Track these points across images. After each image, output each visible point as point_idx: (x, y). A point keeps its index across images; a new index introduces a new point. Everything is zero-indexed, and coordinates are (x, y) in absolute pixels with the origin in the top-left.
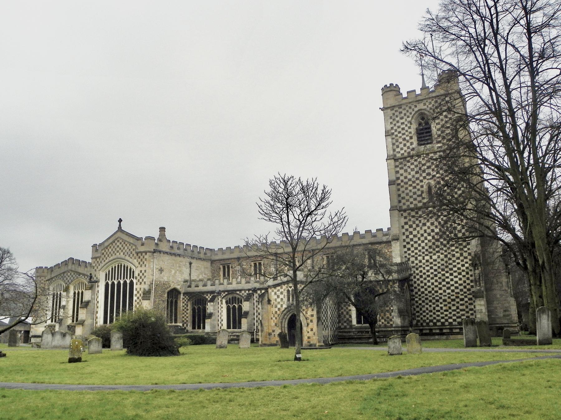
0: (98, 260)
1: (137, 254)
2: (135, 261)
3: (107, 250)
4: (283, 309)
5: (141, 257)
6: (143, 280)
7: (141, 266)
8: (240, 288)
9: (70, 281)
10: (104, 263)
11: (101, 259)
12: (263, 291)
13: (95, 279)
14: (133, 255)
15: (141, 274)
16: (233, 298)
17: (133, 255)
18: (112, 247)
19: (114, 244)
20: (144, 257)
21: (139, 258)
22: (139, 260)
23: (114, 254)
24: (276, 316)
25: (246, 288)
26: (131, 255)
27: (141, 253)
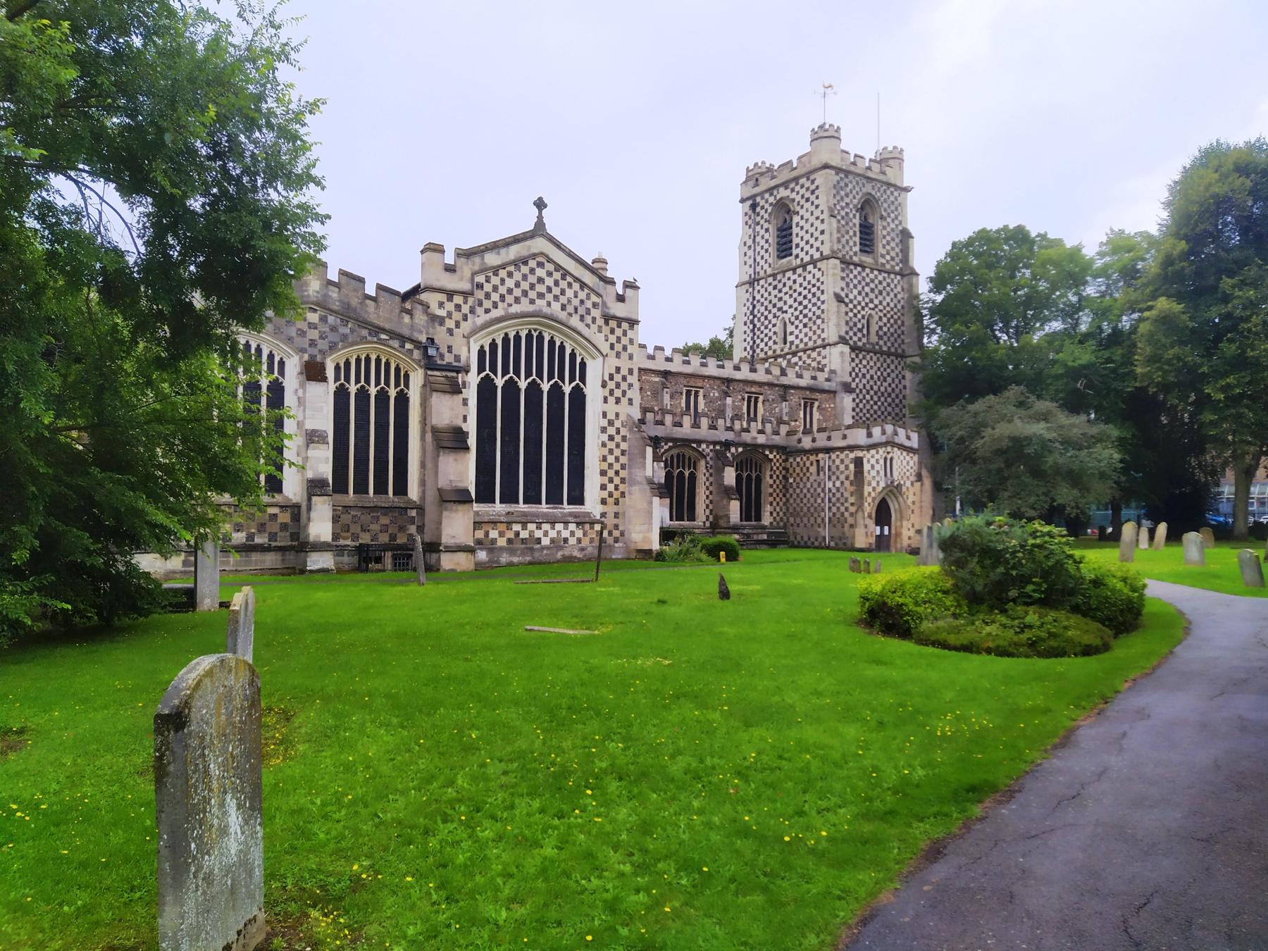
0: (458, 299)
1: (607, 323)
4: (879, 489)
5: (619, 332)
6: (624, 393)
8: (697, 437)
9: (323, 345)
10: (482, 318)
11: (471, 300)
12: (740, 450)
13: (449, 358)
14: (594, 320)
15: (618, 378)
17: (594, 320)
18: (517, 276)
19: (525, 269)
20: (625, 334)
21: (612, 331)
22: (613, 339)
23: (524, 301)
24: (870, 500)
25: (710, 439)
27: (620, 321)
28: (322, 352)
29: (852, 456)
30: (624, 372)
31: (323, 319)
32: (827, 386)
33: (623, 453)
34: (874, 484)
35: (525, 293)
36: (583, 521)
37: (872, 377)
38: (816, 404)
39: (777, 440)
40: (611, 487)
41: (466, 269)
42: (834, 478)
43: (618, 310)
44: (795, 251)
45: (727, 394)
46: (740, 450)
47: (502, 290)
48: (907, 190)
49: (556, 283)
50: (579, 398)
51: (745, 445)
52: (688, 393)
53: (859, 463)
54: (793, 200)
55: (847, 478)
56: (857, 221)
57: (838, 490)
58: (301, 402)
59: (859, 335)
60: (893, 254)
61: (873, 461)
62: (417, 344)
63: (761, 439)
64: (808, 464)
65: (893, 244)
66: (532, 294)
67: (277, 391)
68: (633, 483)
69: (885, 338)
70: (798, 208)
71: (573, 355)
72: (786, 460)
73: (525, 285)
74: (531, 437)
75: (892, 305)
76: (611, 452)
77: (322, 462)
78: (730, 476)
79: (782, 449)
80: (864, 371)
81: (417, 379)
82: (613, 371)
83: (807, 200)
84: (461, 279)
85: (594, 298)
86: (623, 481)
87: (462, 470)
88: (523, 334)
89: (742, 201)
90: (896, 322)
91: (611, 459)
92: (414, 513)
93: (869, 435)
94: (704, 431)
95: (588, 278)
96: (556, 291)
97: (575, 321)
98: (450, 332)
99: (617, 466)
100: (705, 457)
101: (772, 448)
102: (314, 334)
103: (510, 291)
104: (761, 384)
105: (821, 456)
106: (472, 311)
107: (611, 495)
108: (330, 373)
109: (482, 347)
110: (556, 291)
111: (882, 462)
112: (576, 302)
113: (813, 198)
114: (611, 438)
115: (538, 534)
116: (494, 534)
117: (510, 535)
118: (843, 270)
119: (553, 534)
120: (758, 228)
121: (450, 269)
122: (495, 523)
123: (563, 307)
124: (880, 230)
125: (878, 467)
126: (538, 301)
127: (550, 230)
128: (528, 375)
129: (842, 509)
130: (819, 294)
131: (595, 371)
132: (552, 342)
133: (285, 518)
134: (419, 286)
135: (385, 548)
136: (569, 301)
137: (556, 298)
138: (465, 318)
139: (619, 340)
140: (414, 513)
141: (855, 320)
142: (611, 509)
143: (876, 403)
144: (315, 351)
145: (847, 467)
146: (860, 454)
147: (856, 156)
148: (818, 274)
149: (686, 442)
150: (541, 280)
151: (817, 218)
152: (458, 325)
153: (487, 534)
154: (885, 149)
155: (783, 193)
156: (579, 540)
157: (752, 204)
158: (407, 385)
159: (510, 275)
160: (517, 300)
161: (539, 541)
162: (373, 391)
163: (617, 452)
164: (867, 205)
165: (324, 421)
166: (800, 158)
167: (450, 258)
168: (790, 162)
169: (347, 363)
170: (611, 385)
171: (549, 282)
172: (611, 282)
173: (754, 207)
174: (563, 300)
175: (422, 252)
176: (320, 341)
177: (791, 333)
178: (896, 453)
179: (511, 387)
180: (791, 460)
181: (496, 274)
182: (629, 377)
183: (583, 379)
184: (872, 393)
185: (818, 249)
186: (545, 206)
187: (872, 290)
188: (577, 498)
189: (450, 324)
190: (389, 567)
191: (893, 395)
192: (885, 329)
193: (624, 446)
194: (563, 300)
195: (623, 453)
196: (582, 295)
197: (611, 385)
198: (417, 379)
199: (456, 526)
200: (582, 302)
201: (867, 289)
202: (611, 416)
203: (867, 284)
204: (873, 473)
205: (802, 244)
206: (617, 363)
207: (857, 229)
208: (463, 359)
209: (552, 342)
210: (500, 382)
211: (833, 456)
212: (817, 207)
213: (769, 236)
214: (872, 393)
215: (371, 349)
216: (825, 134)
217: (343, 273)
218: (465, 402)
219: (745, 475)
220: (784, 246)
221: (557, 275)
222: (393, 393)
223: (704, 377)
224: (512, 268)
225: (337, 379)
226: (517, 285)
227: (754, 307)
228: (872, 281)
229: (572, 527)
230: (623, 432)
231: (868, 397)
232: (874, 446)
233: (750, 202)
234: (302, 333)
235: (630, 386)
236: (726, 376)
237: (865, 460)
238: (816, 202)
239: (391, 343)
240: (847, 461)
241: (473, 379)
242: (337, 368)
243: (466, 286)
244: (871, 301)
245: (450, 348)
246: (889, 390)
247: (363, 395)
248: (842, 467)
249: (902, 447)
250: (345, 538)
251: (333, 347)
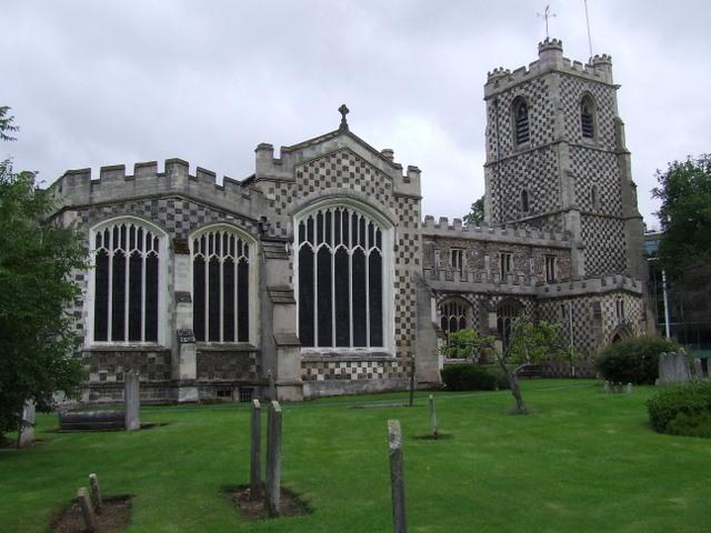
1: (397, 200)
2: (393, 210)
3: (312, 170)
5: (406, 206)
7: (406, 224)
8: (466, 289)
9: (186, 225)
10: (302, 200)
11: (294, 187)
12: (500, 298)
13: (278, 232)
14: (387, 197)
15: (407, 243)
16: (451, 304)
18: (328, 166)
19: (333, 160)
20: (411, 208)
21: (401, 206)
22: (401, 212)
24: (606, 336)
25: (476, 290)
26: (383, 197)
27: (407, 197)
28: (185, 231)
29: (590, 300)
30: (411, 238)
31: (186, 206)
32: (563, 244)
33: (412, 303)
34: (609, 323)
35: (334, 179)
36: (383, 360)
37: (598, 236)
38: (556, 259)
39: (530, 290)
40: (404, 332)
41: (289, 161)
42: (576, 319)
43: (406, 189)
44: (531, 137)
45: (483, 254)
46: (500, 298)
47: (317, 177)
48: (616, 87)
49: (357, 170)
50: (376, 260)
51: (504, 295)
52: (454, 252)
53: (597, 305)
54: (528, 97)
55: (588, 319)
56: (579, 112)
57: (580, 329)
58: (171, 270)
59: (587, 202)
60: (609, 137)
61: (608, 305)
62: (254, 222)
63: (516, 290)
64: (555, 308)
65: (608, 130)
66: (339, 179)
67: (153, 261)
68: (420, 327)
69: (607, 204)
70: (532, 104)
71: (371, 226)
72: (537, 306)
73: (334, 173)
74: (340, 295)
75: (611, 177)
76: (403, 302)
77: (186, 315)
78: (493, 320)
79: (533, 297)
80: (591, 231)
81: (254, 250)
82: (402, 237)
83: (539, 97)
84: (286, 170)
85: (386, 181)
86: (413, 326)
87: (289, 320)
88: (333, 211)
89: (486, 99)
90: (614, 191)
91: (403, 309)
92: (254, 356)
93: (604, 284)
94: (470, 285)
95: (381, 165)
96: (357, 176)
97: (372, 199)
98: (279, 211)
99: (408, 314)
100: (472, 305)
101: (525, 296)
102: (179, 217)
103: (323, 178)
104: (512, 244)
105: (565, 302)
106: (294, 194)
107: (404, 337)
108: (191, 247)
109: (302, 222)
110: (357, 176)
111: (615, 304)
112: (372, 184)
113: (543, 95)
114: (403, 291)
115: (349, 371)
116: (314, 371)
117: (327, 371)
118: (571, 151)
119: (360, 371)
120: (500, 119)
121: (277, 163)
122: (315, 362)
123: (363, 189)
124: (597, 120)
125: (611, 309)
126: (344, 185)
127: (352, 129)
128: (337, 243)
129: (585, 344)
130: (552, 170)
131: (389, 238)
132: (355, 217)
133: (159, 361)
134: (253, 177)
135: (233, 385)
136: (367, 184)
137: (358, 181)
138: (290, 201)
139: (406, 212)
140: (254, 356)
141: (583, 190)
142: (405, 350)
143: (602, 257)
144: (179, 230)
145: (587, 310)
146: (597, 299)
147: (575, 62)
148: (551, 155)
149: (457, 294)
150: (346, 168)
151: (548, 111)
152: (284, 206)
153: (309, 372)
154: (597, 56)
155: (519, 92)
156: (380, 375)
157: (492, 99)
158: (247, 255)
159: (323, 165)
160: (328, 185)
161: (349, 376)
162: (222, 259)
163: (408, 303)
164: (587, 101)
165: (187, 284)
166: (531, 65)
167: (277, 155)
168: (524, 68)
169: (203, 239)
170: (401, 249)
171: (352, 169)
172: (398, 167)
173: (496, 102)
174: (363, 183)
175: (256, 151)
176: (184, 223)
177: (532, 202)
178: (626, 297)
179: (324, 252)
180: (540, 306)
181: (311, 165)
182: (415, 242)
183: (379, 245)
184: (599, 249)
185: (550, 135)
186: (348, 111)
187: (595, 167)
188: (377, 341)
189: (278, 205)
190: (237, 399)
191: (616, 251)
192: (606, 197)
193: (413, 297)
194: (363, 183)
195: (412, 303)
196: (377, 178)
197: (401, 249)
198: (254, 250)
199: (289, 365)
200: (377, 184)
201: (590, 166)
202: (402, 274)
203: (591, 162)
204: (609, 314)
205: (536, 131)
206: (406, 231)
207: (580, 118)
208: (288, 232)
209: (355, 217)
210: (316, 249)
211: (576, 301)
212: (548, 102)
213: (509, 125)
214: (599, 249)
215: (220, 227)
216: (550, 48)
217: (199, 170)
218: (291, 265)
219: (504, 319)
220: (521, 134)
221: (358, 164)
222: (236, 261)
223: (466, 240)
224: (323, 160)
225: (196, 251)
226: (328, 173)
227: (500, 181)
228: (594, 159)
229: (374, 365)
230: (412, 286)
231: (596, 253)
232: (608, 293)
233: (491, 101)
234: (171, 217)
235: (416, 248)
236: (483, 238)
237: (601, 304)
238: (546, 98)
239: (235, 221)
240: (587, 305)
241: (296, 247)
242: (196, 243)
243: (289, 175)
244: (594, 175)
245: (278, 225)
246: (613, 246)
247: (214, 262)
248: (583, 310)
249: (630, 293)
250: (204, 377)
251: (193, 227)
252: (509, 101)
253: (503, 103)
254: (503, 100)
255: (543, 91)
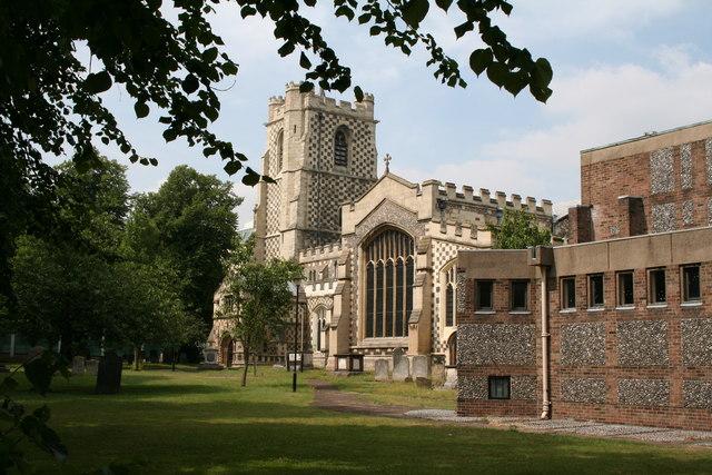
113: (366, 137)
173: (320, 118)
185: (369, 172)
252: (334, 124)
253: (327, 122)
254: (327, 119)
255: (366, 133)
